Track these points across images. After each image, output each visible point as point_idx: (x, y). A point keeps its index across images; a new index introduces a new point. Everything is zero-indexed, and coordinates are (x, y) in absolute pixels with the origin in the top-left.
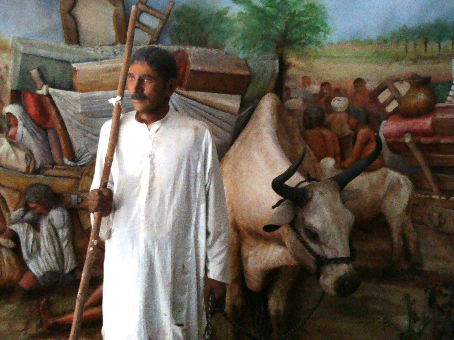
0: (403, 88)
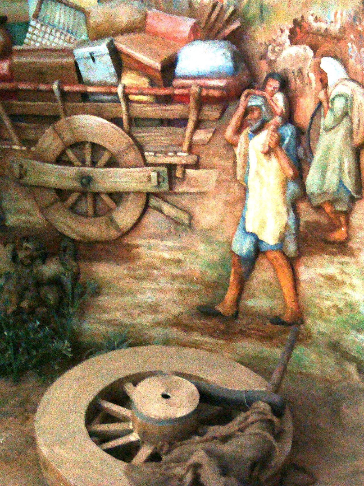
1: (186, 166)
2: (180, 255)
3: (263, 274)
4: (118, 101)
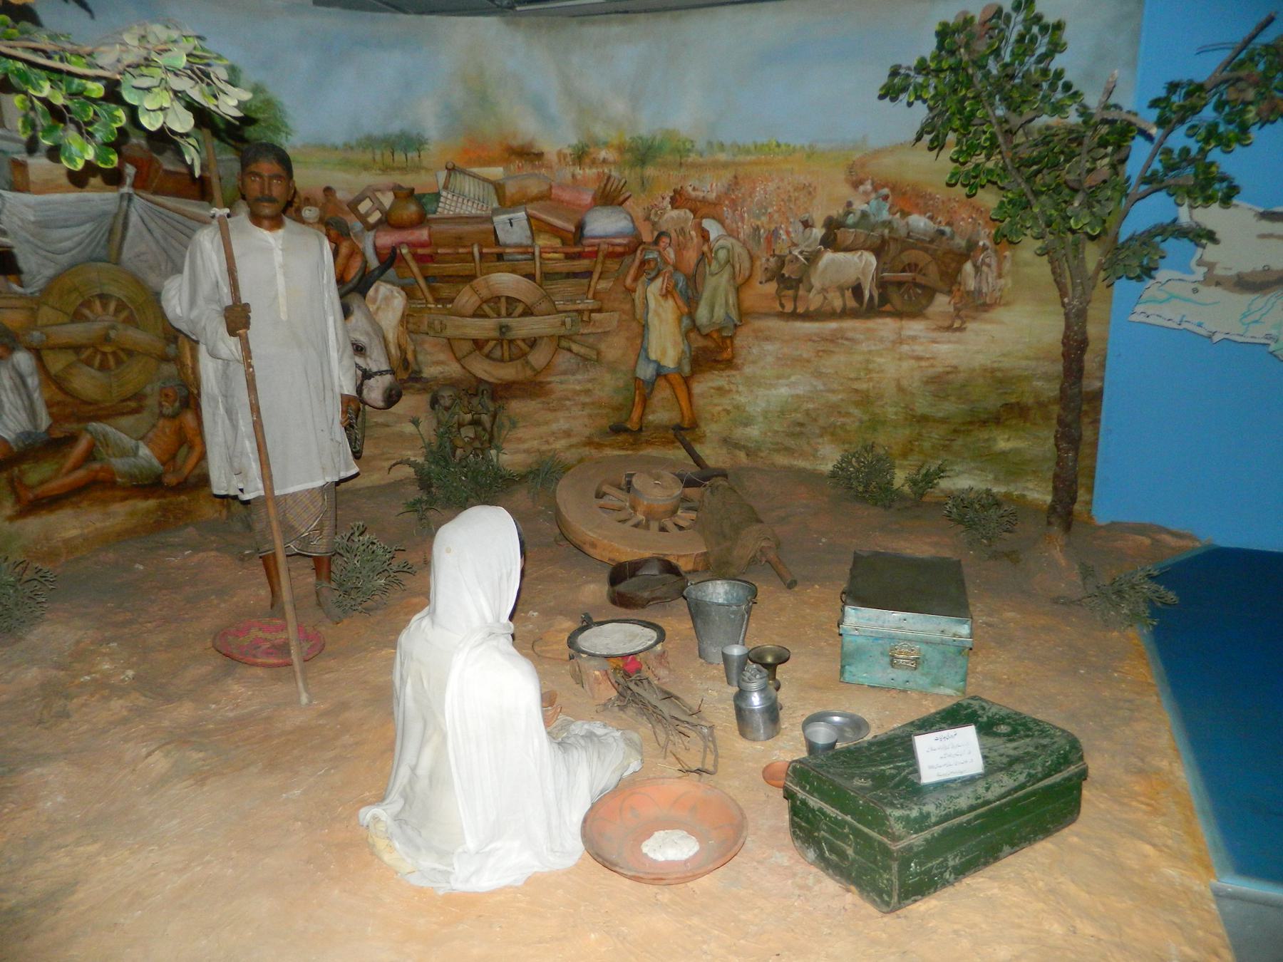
0: (387, 200)
1: (592, 311)
2: (590, 386)
3: (662, 393)
4: (533, 259)
